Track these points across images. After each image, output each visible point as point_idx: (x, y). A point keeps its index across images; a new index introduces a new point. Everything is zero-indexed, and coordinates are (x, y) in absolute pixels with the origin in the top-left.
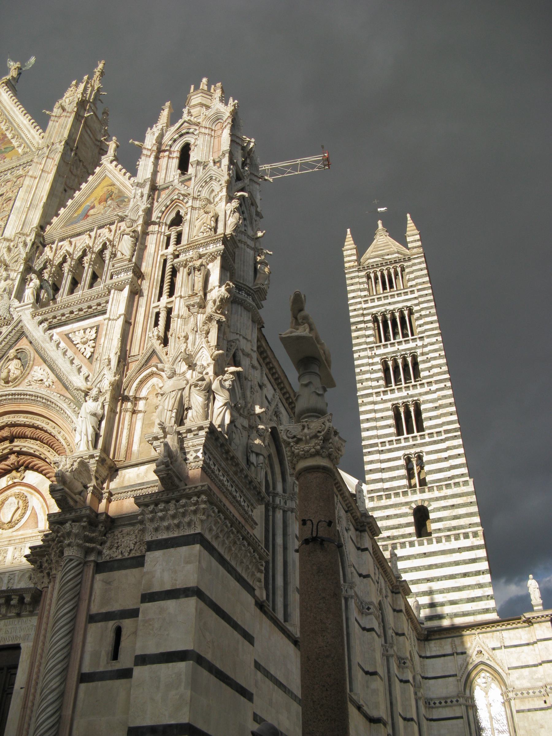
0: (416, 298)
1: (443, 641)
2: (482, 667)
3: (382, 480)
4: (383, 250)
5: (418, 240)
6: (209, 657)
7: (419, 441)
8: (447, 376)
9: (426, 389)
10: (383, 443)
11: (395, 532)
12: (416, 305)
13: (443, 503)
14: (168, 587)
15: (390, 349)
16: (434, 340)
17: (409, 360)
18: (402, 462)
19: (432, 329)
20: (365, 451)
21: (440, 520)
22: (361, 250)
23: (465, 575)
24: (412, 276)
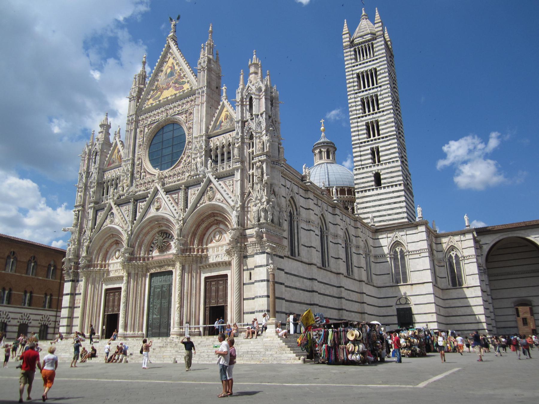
0: (378, 63)
1: (382, 232)
3: (361, 161)
4: (363, 31)
5: (380, 27)
9: (381, 114)
10: (361, 143)
11: (366, 185)
12: (379, 67)
14: (260, 264)
16: (386, 87)
17: (374, 98)
18: (369, 151)
20: (353, 147)
21: (385, 178)
22: (351, 32)
23: (395, 203)
24: (377, 49)
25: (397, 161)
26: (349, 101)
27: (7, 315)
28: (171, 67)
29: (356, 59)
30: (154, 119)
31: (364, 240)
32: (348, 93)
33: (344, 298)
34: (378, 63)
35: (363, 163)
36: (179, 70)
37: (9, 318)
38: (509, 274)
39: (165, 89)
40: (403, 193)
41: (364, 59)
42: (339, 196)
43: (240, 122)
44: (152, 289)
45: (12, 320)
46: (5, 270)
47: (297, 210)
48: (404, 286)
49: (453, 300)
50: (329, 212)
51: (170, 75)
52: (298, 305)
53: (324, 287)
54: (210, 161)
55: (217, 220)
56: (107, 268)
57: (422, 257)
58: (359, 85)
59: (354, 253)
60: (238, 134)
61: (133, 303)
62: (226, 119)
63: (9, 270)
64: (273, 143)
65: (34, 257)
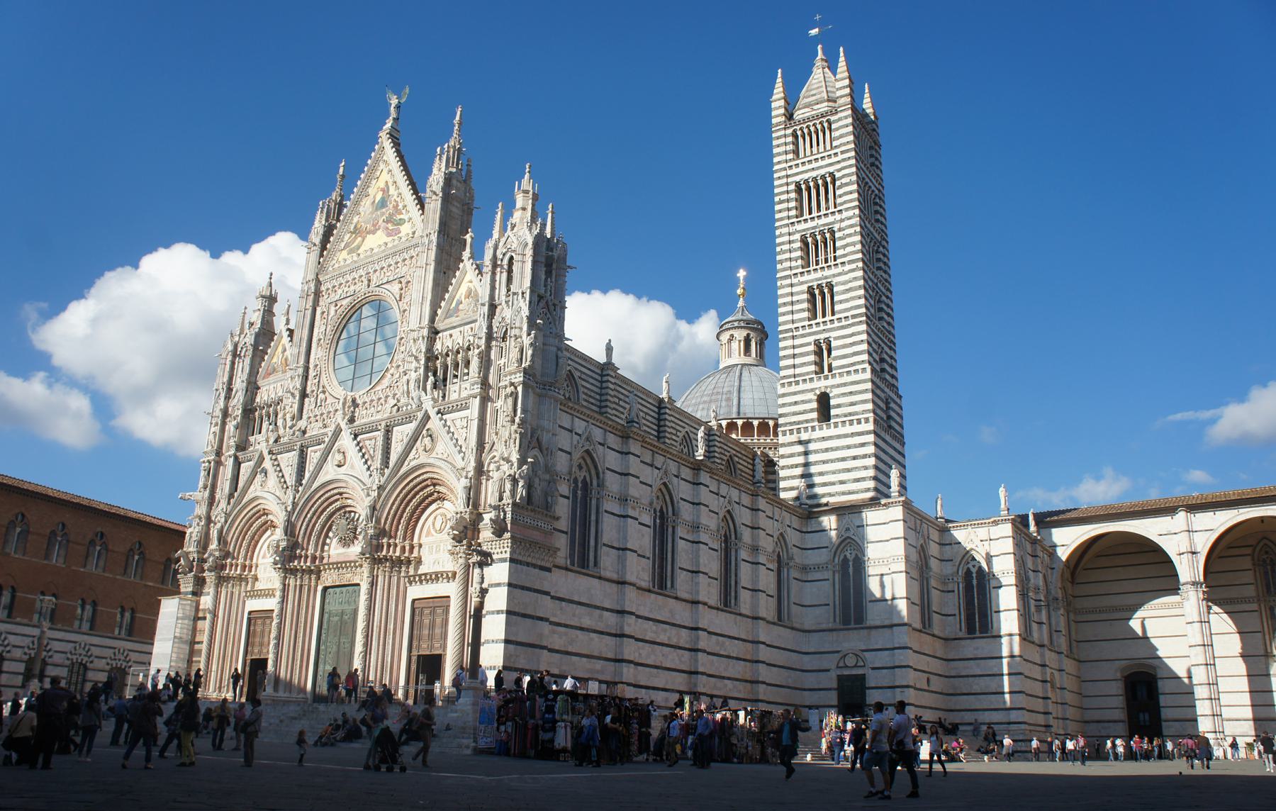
0: (839, 162)
2: (849, 540)
6: (517, 610)
7: (829, 326)
8: (860, 255)
9: (840, 269)
12: (839, 170)
15: (810, 224)
16: (850, 213)
17: (828, 235)
18: (812, 348)
19: (851, 201)
20: (781, 336)
21: (839, 406)
23: (855, 458)
25: (864, 370)
26: (778, 241)
27: (86, 649)
28: (383, 190)
29: (796, 152)
30: (346, 289)
31: (776, 534)
32: (777, 224)
33: (704, 651)
35: (798, 371)
36: (395, 197)
37: (91, 656)
39: (369, 233)
40: (871, 438)
41: (812, 154)
42: (756, 437)
43: (487, 304)
44: (326, 616)
45: (96, 660)
46: (85, 566)
47: (598, 477)
48: (855, 632)
49: (966, 662)
50: (682, 479)
51: (380, 204)
52: (584, 660)
53: (654, 628)
54: (431, 379)
55: (439, 492)
56: (253, 573)
57: (893, 573)
58: (800, 208)
59: (743, 560)
60: (480, 326)
61: (290, 641)
62: (468, 296)
63: (91, 567)
64: (545, 347)
65: (140, 543)
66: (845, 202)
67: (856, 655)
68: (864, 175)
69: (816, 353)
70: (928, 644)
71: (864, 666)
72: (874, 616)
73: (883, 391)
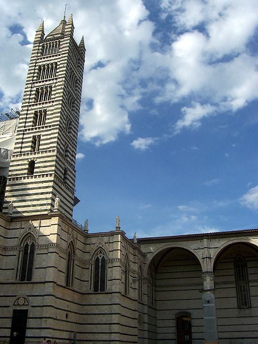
0: (60, 58)
7: (41, 130)
9: (51, 104)
10: (26, 130)
12: (59, 62)
13: (42, 160)
21: (38, 167)
23: (42, 194)
24: (62, 46)
34: (60, 58)
35: (23, 150)
38: (175, 286)
66: (59, 75)
67: (25, 298)
68: (72, 67)
69: (32, 142)
70: (68, 295)
71: (28, 305)
72: (37, 276)
73: (64, 164)
